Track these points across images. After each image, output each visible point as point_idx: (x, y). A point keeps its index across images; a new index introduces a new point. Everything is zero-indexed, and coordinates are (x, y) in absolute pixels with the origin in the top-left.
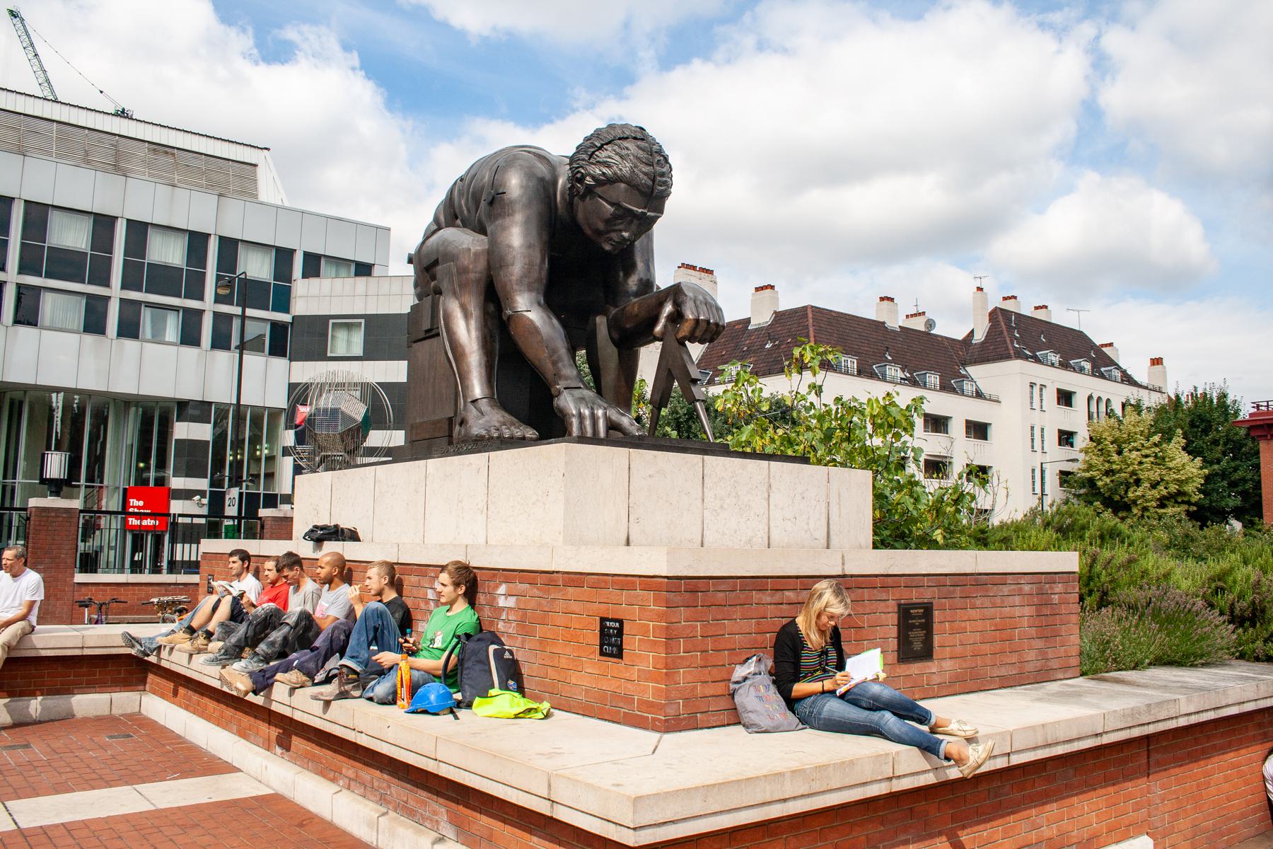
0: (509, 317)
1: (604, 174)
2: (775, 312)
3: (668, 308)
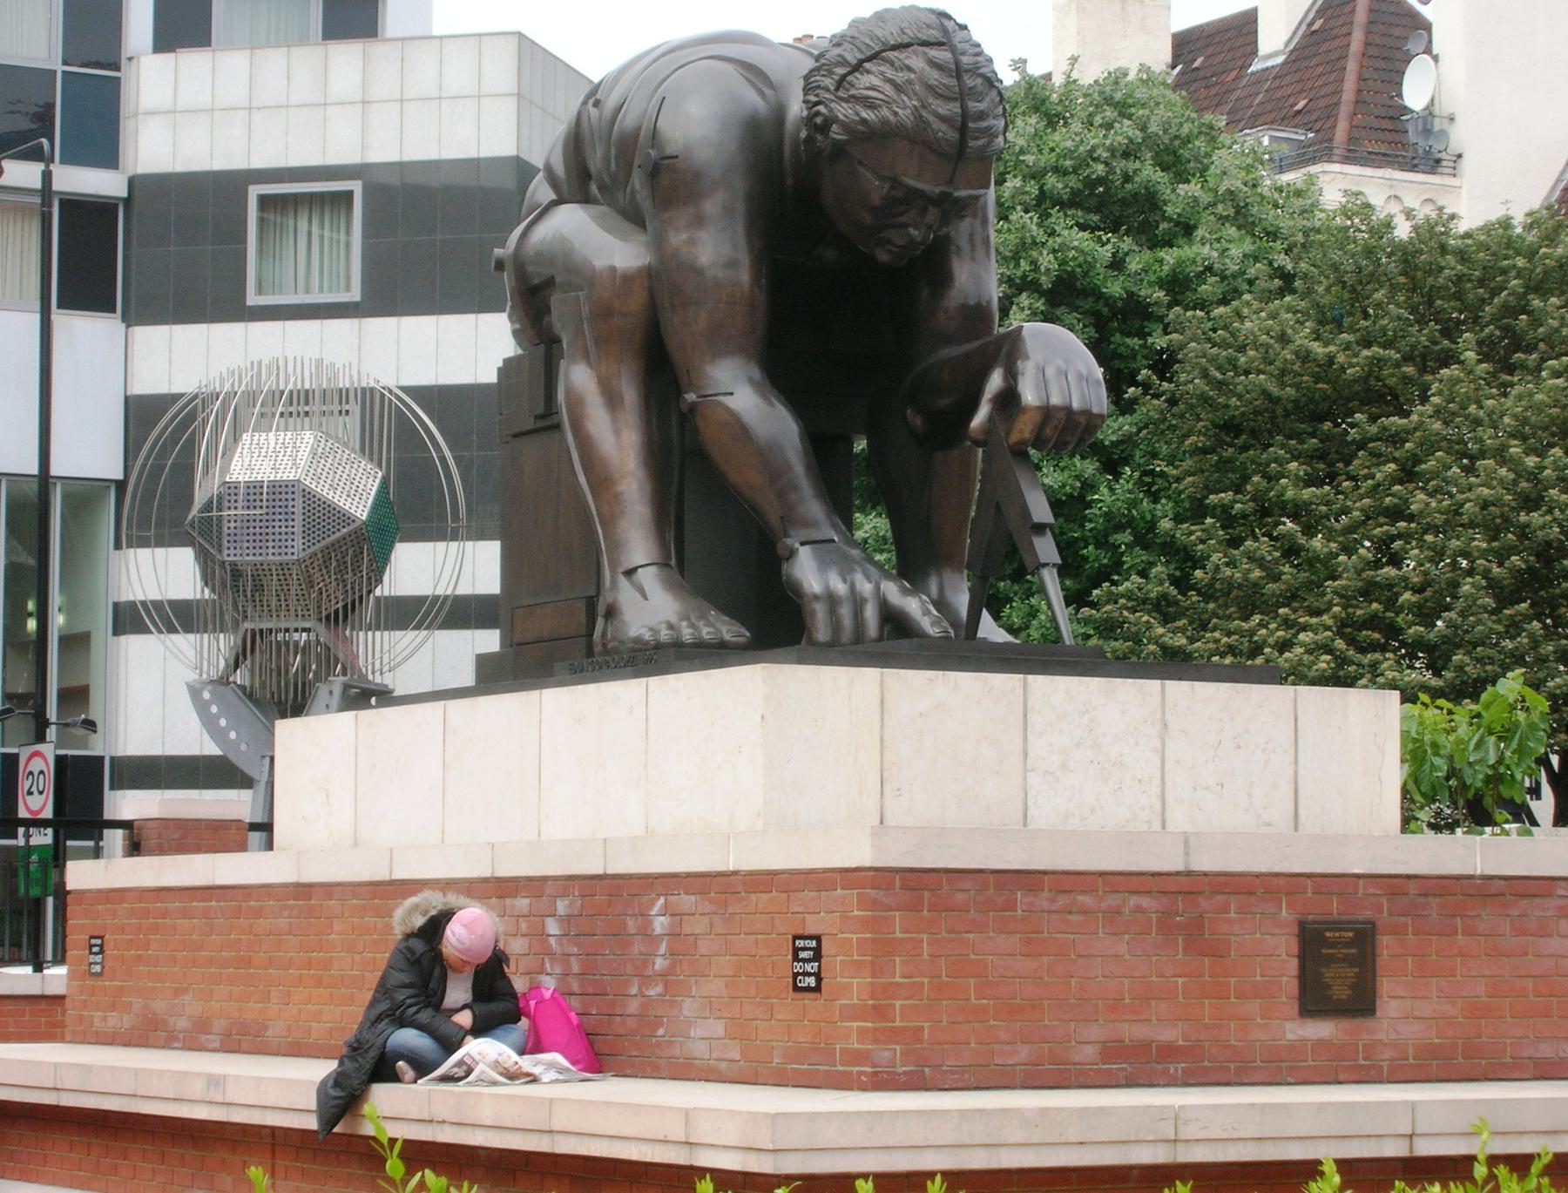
0: (693, 407)
1: (864, 121)
3: (995, 381)
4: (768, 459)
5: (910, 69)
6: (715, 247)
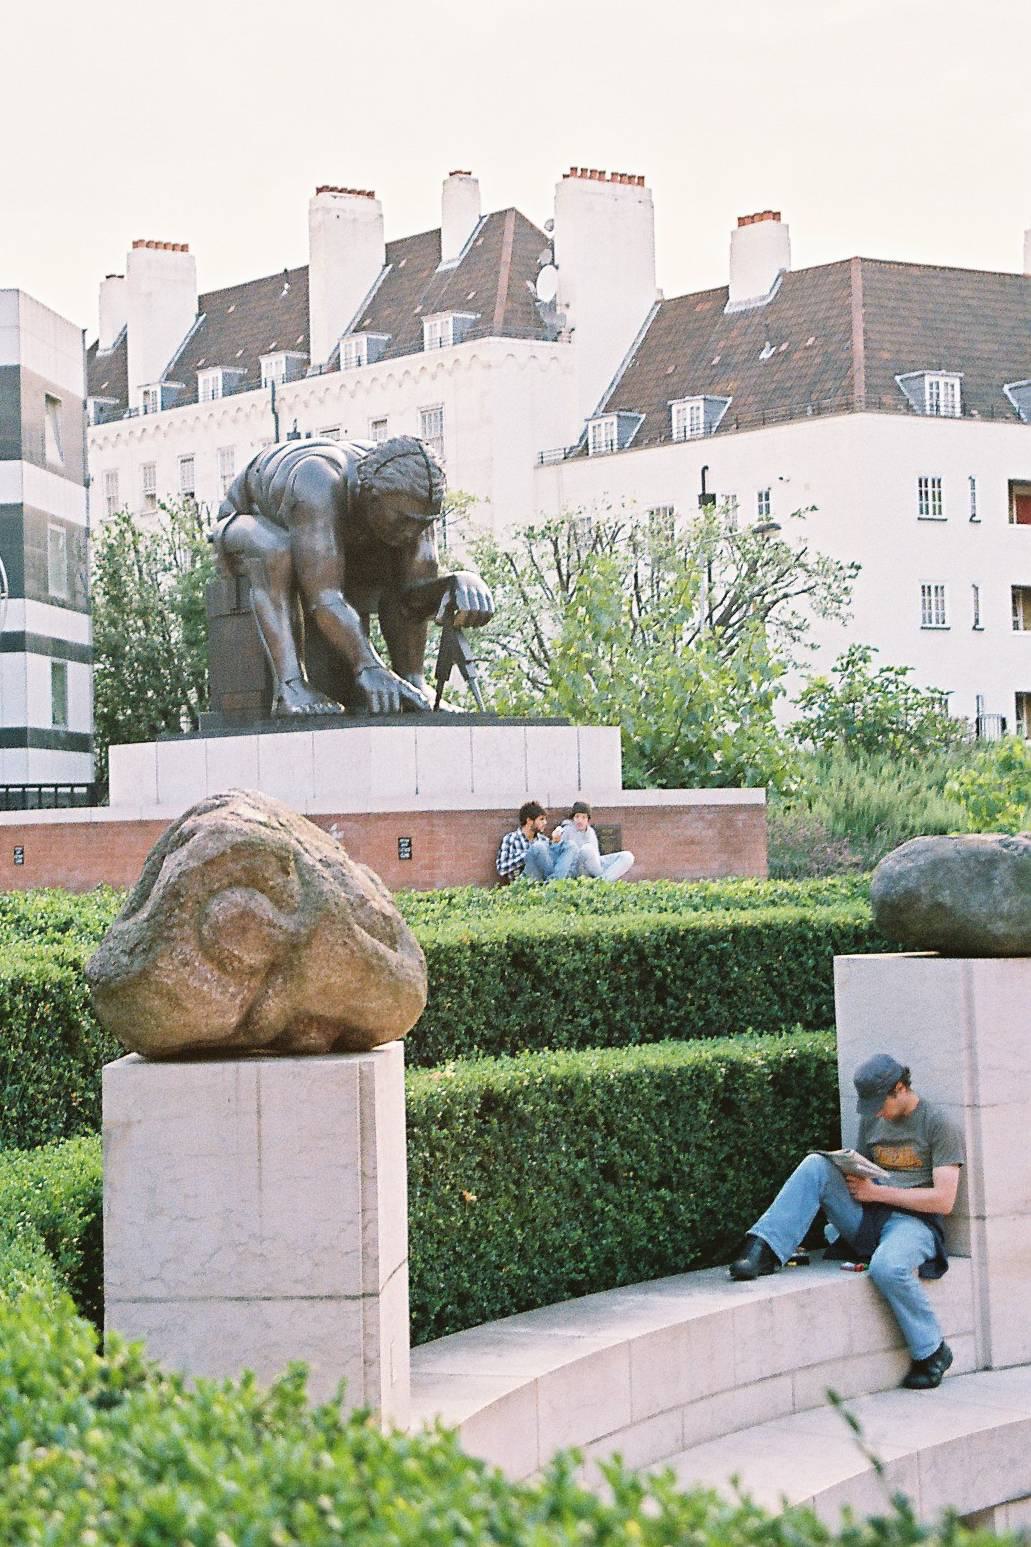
2: (783, 274)
3: (445, 601)
4: (348, 632)
5: (405, 465)
6: (322, 542)
